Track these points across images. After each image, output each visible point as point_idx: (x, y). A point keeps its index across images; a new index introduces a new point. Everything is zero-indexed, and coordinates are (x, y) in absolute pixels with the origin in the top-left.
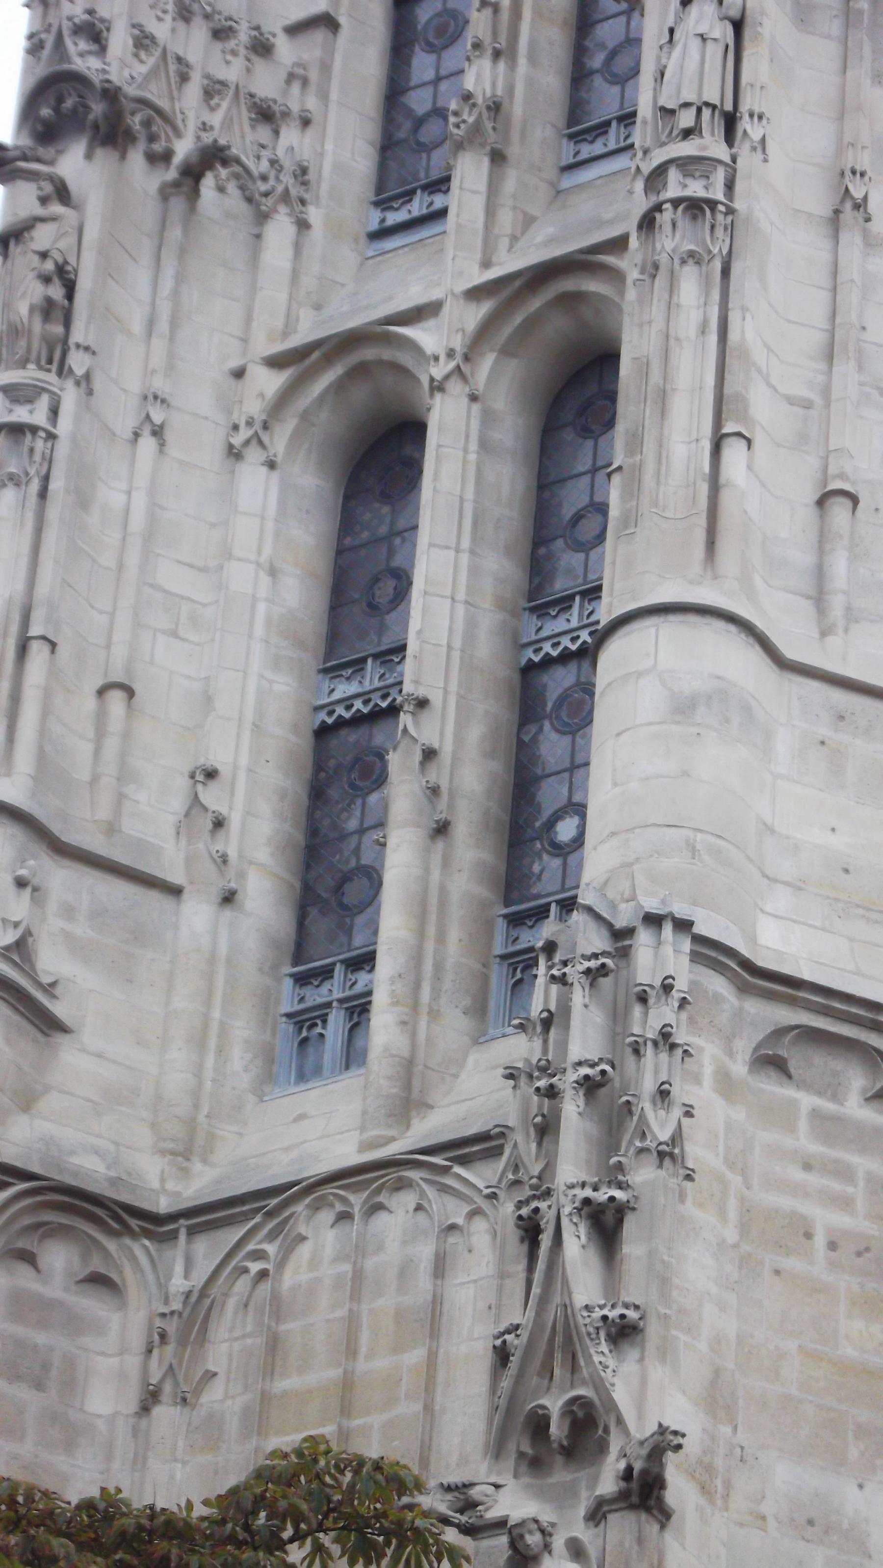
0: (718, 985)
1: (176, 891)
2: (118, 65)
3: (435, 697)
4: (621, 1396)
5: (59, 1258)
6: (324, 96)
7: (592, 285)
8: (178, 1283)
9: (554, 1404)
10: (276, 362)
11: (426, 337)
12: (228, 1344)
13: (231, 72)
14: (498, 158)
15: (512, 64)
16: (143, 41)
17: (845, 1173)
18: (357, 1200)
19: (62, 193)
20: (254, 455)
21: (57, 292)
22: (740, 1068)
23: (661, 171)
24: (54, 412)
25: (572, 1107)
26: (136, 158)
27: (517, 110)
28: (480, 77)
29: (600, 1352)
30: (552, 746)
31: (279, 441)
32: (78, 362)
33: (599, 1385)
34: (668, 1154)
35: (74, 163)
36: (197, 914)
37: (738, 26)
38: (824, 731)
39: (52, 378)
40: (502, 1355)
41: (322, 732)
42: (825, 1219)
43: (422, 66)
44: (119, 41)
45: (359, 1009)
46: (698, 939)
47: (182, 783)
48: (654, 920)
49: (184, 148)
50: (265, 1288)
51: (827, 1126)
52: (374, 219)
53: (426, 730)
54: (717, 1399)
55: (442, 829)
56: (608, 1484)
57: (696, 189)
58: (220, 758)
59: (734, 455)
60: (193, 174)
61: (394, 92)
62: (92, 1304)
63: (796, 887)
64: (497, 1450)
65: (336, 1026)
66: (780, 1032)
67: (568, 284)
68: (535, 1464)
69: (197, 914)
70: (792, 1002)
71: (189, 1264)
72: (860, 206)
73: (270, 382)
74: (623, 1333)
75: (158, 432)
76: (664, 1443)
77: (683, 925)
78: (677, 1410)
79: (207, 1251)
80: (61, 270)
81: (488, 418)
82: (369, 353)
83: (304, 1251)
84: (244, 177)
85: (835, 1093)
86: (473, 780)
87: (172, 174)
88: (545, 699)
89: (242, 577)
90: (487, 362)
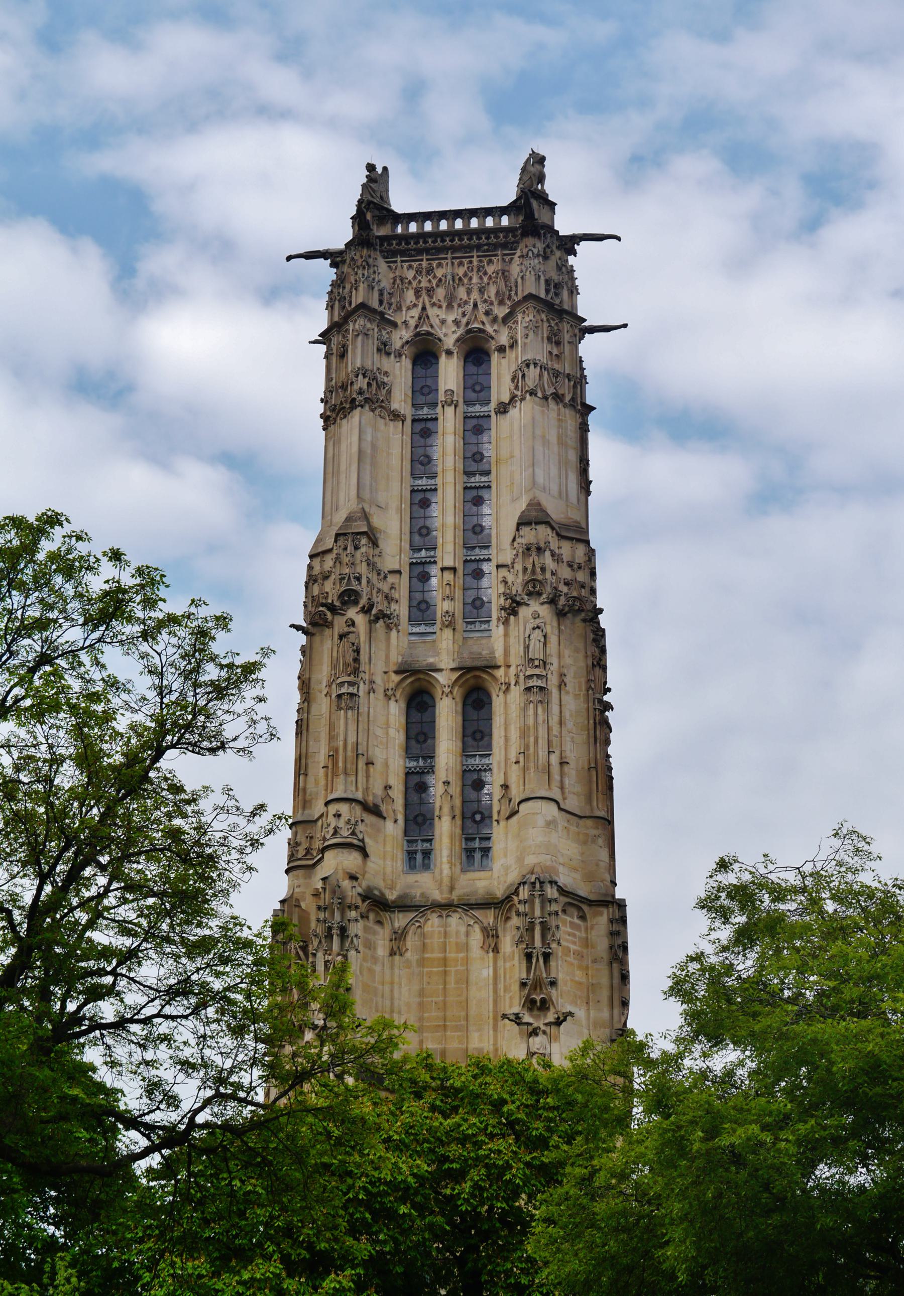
7: (485, 676)
10: (396, 672)
12: (411, 941)
18: (444, 913)
20: (393, 698)
37: (545, 636)
51: (572, 924)
55: (454, 817)
62: (377, 928)
67: (478, 673)
68: (530, 1010)
69: (389, 824)
71: (400, 920)
74: (553, 983)
82: (422, 676)
83: (430, 922)
90: (456, 689)
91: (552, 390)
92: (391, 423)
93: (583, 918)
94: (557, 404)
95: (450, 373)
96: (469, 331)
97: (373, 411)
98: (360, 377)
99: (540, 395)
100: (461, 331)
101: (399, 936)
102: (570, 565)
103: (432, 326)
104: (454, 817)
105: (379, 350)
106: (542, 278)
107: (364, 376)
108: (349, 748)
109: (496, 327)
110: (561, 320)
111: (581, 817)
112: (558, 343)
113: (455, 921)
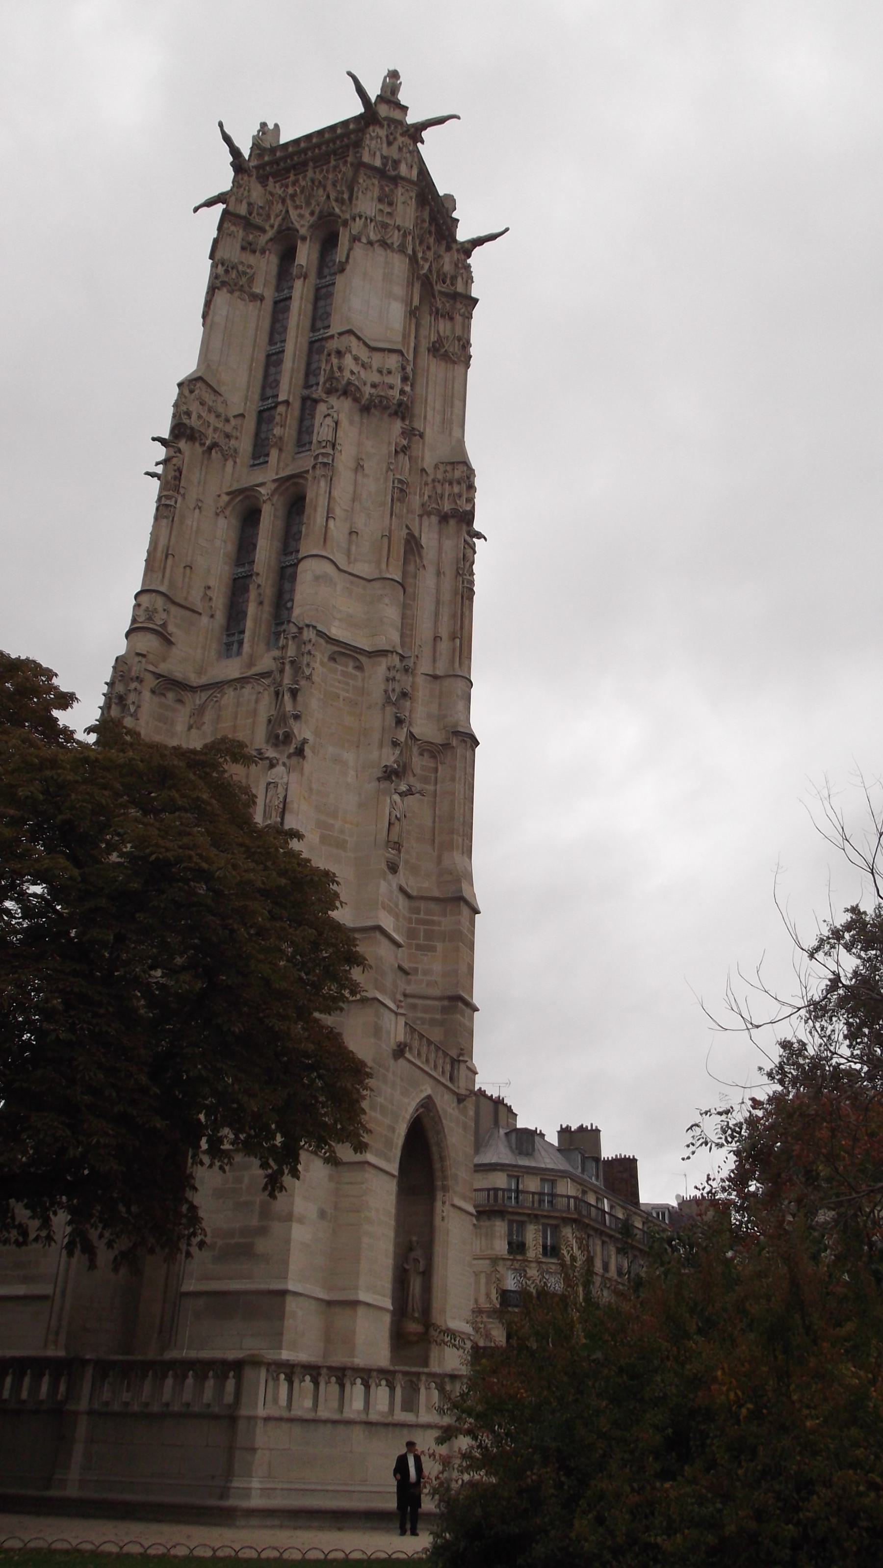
0: (322, 641)
1: (200, 614)
2: (194, 422)
3: (261, 573)
4: (296, 731)
5: (171, 695)
6: (241, 432)
7: (301, 481)
8: (198, 702)
9: (281, 732)
10: (228, 494)
11: (262, 490)
12: (208, 717)
13: (220, 425)
14: (281, 450)
15: (285, 429)
16: (200, 417)
17: (348, 684)
18: (238, 686)
19: (180, 451)
20: (221, 515)
21: (177, 474)
22: (326, 660)
23: (318, 455)
24: (176, 502)
25: (287, 667)
26: (197, 444)
27: (286, 439)
28: (277, 431)
29: (292, 721)
30: (287, 586)
31: (227, 512)
32: (182, 491)
33: (291, 728)
34: (309, 678)
35: (182, 444)
36: (205, 620)
37: (336, 423)
38: (348, 585)
39: (175, 494)
40: (270, 721)
41: (235, 580)
42: (343, 694)
43: (264, 427)
44: (194, 416)
45: (241, 643)
46: (318, 631)
47: (202, 589)
48: (308, 626)
49: (208, 443)
50: (218, 704)
51: (345, 674)
52: (251, 463)
53: (259, 580)
54: (317, 733)
55: (261, 603)
56: (292, 750)
57: (325, 460)
58: (211, 584)
59: (331, 523)
60: (210, 449)
61: (257, 434)
62: (178, 706)
63: (340, 620)
64: (267, 742)
65: (235, 647)
66: (335, 652)
67: (296, 480)
68: (276, 745)
69: (205, 620)
70: (338, 646)
71: (199, 699)
72: (362, 467)
73: (226, 498)
74: (297, 717)
75: (200, 508)
76: (305, 741)
77: (314, 627)
78: (308, 735)
79: (204, 696)
80: (178, 469)
81: (276, 509)
83: (226, 696)
84: (222, 450)
85: (346, 666)
86: (269, 592)
87: (205, 448)
88: (286, 575)
89: (218, 543)
91: (379, 237)
92: (252, 303)
93: (360, 668)
94: (386, 250)
95: (306, 255)
96: (320, 218)
97: (231, 292)
98: (220, 266)
99: (364, 240)
100: (313, 219)
101: (200, 711)
102: (380, 371)
103: (292, 223)
104: (261, 603)
105: (243, 249)
106: (378, 154)
107: (223, 264)
108: (160, 549)
109: (344, 208)
110: (396, 185)
111: (369, 581)
112: (390, 204)
113: (247, 691)
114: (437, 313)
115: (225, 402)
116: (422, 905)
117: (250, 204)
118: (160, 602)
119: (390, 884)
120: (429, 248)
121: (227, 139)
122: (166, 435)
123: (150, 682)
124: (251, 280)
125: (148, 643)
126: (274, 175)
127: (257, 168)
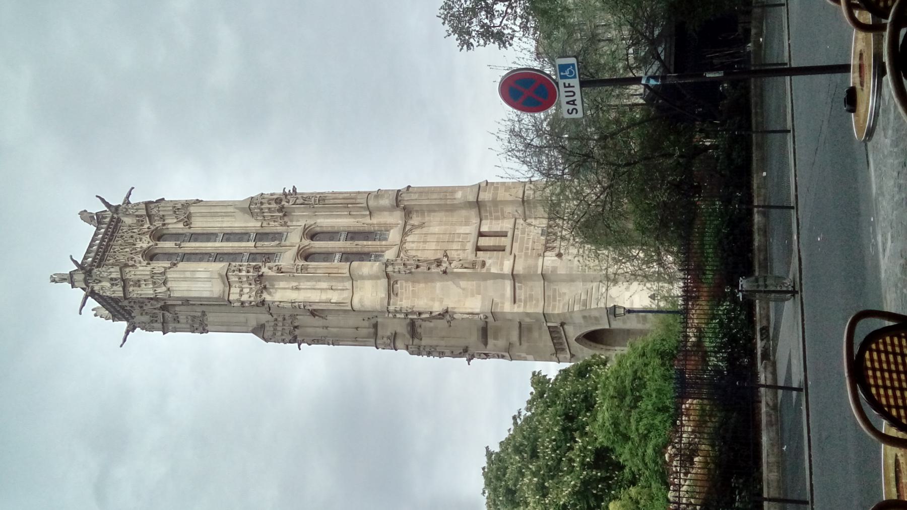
5: (419, 330)
51: (402, 289)
69: (379, 320)
97: (207, 325)
114: (164, 225)
115: (268, 322)
116: (483, 214)
117: (152, 322)
118: (379, 342)
119: (490, 265)
120: (132, 237)
121: (125, 340)
122: (296, 345)
123: (416, 341)
124: (194, 317)
125: (399, 343)
126: (130, 314)
127: (127, 320)
